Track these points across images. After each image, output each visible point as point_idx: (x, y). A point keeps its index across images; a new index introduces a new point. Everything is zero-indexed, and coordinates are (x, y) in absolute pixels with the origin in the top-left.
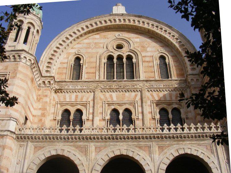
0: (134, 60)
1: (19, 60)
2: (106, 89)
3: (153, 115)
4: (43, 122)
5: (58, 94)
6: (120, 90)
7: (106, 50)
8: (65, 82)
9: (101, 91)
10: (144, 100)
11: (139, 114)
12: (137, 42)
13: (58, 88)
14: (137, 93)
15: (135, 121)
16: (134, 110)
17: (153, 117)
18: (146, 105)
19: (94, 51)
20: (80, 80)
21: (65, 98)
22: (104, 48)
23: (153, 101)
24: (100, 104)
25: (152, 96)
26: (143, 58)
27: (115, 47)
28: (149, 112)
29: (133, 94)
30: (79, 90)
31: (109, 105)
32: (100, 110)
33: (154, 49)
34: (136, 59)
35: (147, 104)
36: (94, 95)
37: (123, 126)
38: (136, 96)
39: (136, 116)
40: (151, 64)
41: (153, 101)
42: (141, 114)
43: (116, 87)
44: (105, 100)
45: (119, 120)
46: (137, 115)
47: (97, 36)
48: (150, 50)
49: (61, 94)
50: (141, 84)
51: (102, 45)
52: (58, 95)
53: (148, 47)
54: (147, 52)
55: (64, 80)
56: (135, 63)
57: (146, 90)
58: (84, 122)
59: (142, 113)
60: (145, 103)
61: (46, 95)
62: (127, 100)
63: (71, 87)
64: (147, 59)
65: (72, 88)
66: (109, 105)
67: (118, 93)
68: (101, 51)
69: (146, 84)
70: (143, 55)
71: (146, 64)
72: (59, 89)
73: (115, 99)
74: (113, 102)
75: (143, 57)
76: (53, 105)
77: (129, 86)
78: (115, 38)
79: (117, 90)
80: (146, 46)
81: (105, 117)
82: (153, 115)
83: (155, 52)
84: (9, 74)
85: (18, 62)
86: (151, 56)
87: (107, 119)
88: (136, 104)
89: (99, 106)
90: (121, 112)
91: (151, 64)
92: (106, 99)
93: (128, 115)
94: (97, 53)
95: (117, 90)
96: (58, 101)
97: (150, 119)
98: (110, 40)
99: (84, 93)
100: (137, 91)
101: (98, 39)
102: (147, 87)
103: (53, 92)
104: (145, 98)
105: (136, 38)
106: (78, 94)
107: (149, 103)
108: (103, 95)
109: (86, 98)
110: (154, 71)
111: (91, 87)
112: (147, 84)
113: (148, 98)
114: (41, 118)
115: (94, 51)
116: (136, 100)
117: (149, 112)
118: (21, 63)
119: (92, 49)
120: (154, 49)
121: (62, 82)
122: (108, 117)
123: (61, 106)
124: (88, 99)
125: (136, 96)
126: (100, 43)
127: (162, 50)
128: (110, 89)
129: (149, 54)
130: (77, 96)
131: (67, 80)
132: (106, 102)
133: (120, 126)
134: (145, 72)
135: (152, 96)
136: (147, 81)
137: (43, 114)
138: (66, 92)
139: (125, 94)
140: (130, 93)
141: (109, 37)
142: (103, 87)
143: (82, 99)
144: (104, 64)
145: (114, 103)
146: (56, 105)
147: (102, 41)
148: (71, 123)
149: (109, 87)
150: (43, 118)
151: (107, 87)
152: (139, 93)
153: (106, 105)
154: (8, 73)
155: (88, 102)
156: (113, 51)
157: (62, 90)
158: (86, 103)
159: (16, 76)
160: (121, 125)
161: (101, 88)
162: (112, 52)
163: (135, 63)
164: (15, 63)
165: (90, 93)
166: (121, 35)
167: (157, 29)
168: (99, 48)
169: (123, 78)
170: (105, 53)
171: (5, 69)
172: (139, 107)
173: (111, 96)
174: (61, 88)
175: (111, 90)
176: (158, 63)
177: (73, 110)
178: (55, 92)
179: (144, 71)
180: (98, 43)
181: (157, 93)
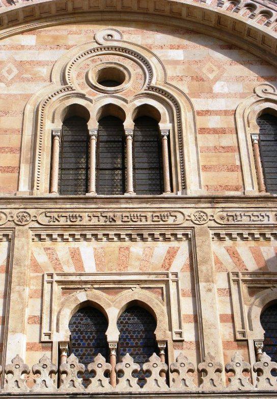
0: (165, 125)
2: (55, 228)
3: (239, 328)
6: (112, 233)
7: (60, 87)
9: (39, 236)
10: (202, 269)
11: (184, 325)
12: (176, 63)
14: (174, 244)
15: (166, 350)
16: (165, 308)
17: (239, 337)
18: (210, 290)
19: (15, 90)
22: (54, 80)
23: (237, 275)
24: (35, 286)
25: (234, 254)
26: (197, 117)
27: (93, 80)
28: (223, 318)
29: (161, 248)
31: (68, 287)
32: (32, 308)
33: (238, 88)
34: (172, 121)
35: (215, 287)
36: (11, 250)
37: (119, 360)
38: (172, 254)
39: (171, 329)
40: (228, 140)
41: (237, 275)
42: (193, 325)
43: (95, 221)
44: (52, 271)
45: (107, 344)
46: (175, 328)
47: (29, 40)
48: (226, 90)
50: (190, 211)
51: (44, 71)
53: (216, 79)
54: (213, 97)
56: (168, 137)
57: (211, 232)
59: (197, 319)
60: (207, 281)
62: (137, 271)
64: (213, 122)
67: (105, 243)
68: (40, 91)
69: (209, 212)
70: (197, 108)
71: (210, 140)
73: (90, 266)
74: (84, 278)
75: (199, 113)
77: (143, 219)
78: (96, 46)
79: (100, 234)
80: (211, 76)
81: (49, 335)
82: (239, 328)
83: (243, 96)
86: (226, 113)
87: (59, 343)
88: (173, 286)
89: (27, 290)
90: (113, 314)
91: (228, 140)
92: (57, 263)
93: (142, 327)
94: (27, 97)
95: (100, 234)
97: (226, 345)
98: (75, 52)
100: (175, 235)
101: (30, 48)
102: (213, 224)
104: (206, 261)
105: (172, 47)
107: (221, 281)
110: (238, 163)
112: (216, 212)
113: (218, 261)
115: (15, 92)
116: (173, 269)
117: (223, 318)
119: (8, 84)
120: (238, 88)
122: (63, 334)
125: (172, 254)
126: (39, 63)
127: (270, 90)
128: (70, 227)
129: (220, 104)
132: (56, 278)
133: (108, 360)
134: (205, 168)
135: (234, 254)
136: (213, 200)
139: (128, 248)
140: (150, 243)
141: (70, 43)
142: (44, 220)
144: (53, 137)
145: (86, 282)
147: (46, 55)
149: (69, 223)
151: (62, 221)
152: (184, 246)
153: (57, 288)
156: (86, 91)
160: (114, 358)
161: (37, 225)
162: (82, 96)
163: (168, 137)
166: (116, 36)
167: (252, 16)
168: (35, 79)
169: (124, 190)
170: (54, 99)
172: (184, 295)
173: (75, 256)
176: (256, 138)
179: (201, 164)
180: (31, 63)
181: (252, 244)
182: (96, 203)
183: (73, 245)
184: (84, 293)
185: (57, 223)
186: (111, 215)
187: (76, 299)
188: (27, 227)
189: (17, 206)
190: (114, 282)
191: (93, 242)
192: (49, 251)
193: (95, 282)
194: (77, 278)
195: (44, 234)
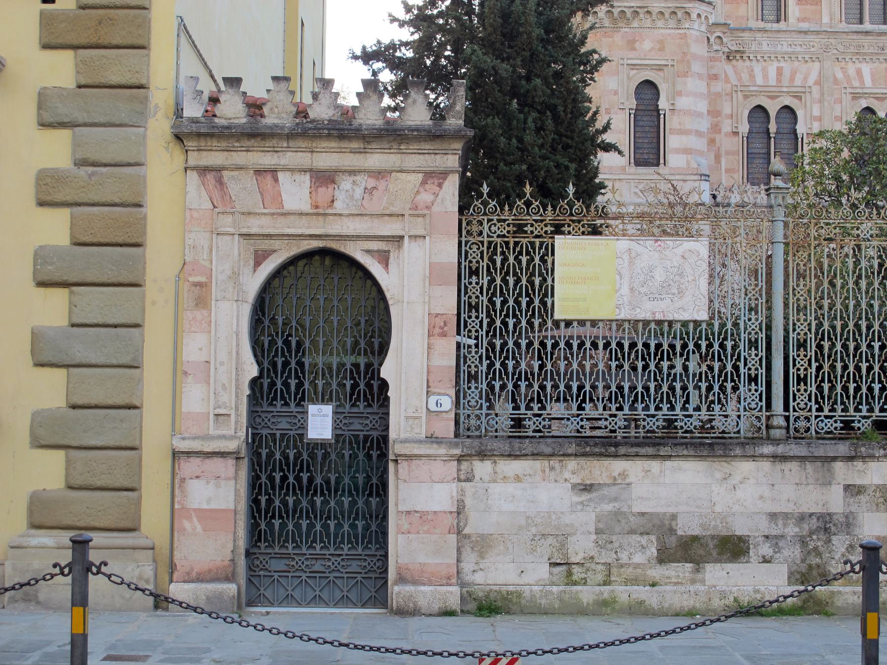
1: (687, 26)
4: (717, 145)
5: (734, 62)
8: (751, 30)
13: (734, 48)
20: (782, 25)
21: (752, 76)
30: (786, 56)
31: (856, 97)
44: (846, 86)
49: (741, 62)
52: (734, 66)
55: (744, 26)
58: (800, 140)
61: (715, 75)
63: (765, 47)
65: (769, 49)
66: (856, 97)
67: (876, 65)
72: (737, 51)
73: (868, 82)
74: (865, 91)
76: (727, 94)
84: (673, 66)
85: (686, 31)
92: (849, 81)
95: (874, 58)
96: (739, 85)
99: (796, 63)
103: (724, 57)
106: (782, 64)
108: (842, 68)
109: (802, 77)
111: (813, 47)
114: (712, 136)
118: (692, 32)
121: (744, 30)
123: (746, 97)
124: (806, 79)
130: (780, 71)
131: (753, 24)
137: (716, 125)
138: (754, 59)
143: (792, 79)
145: (866, 93)
146: (734, 95)
148: (773, 139)
149: (856, 51)
150: (718, 137)
151: (852, 50)
154: (670, 63)
155: (808, 90)
157: (743, 52)
158: (803, 90)
159: (690, 70)
161: (836, 52)
164: (680, 31)
165: (810, 64)
171: (659, 50)
173: (859, 72)
174: (741, 49)
175: (860, 55)
177: (773, 109)
178: (728, 57)
182: (872, 35)
183: (858, 65)
184: (864, 101)
185: (849, 51)
186: (881, 45)
187: (861, 105)
188: (830, 53)
189: (823, 36)
190: (882, 94)
191: (870, 65)
192: (844, 70)
193: (872, 93)
194: (861, 91)
195: (840, 58)
